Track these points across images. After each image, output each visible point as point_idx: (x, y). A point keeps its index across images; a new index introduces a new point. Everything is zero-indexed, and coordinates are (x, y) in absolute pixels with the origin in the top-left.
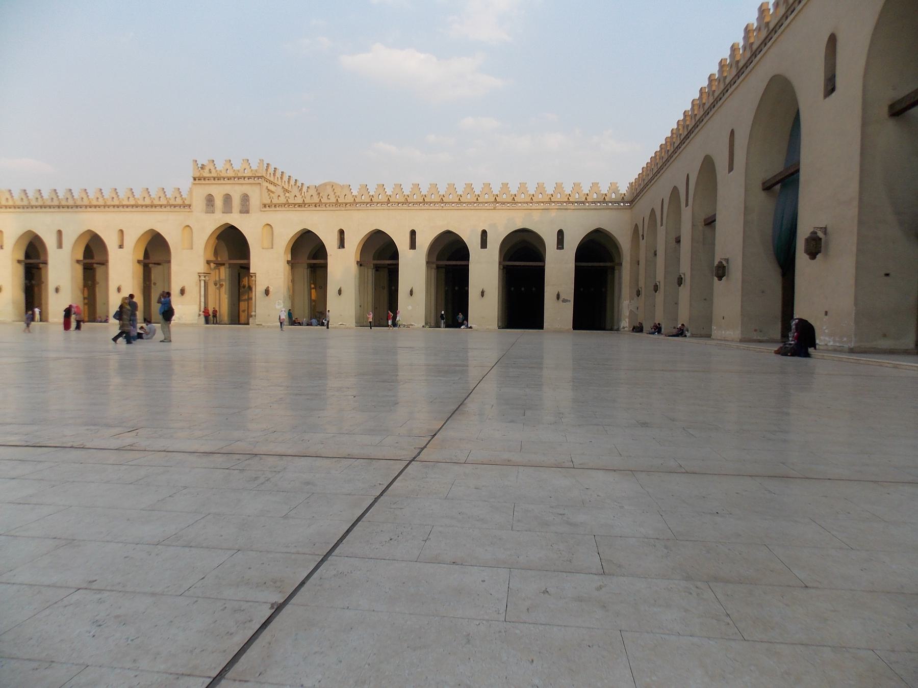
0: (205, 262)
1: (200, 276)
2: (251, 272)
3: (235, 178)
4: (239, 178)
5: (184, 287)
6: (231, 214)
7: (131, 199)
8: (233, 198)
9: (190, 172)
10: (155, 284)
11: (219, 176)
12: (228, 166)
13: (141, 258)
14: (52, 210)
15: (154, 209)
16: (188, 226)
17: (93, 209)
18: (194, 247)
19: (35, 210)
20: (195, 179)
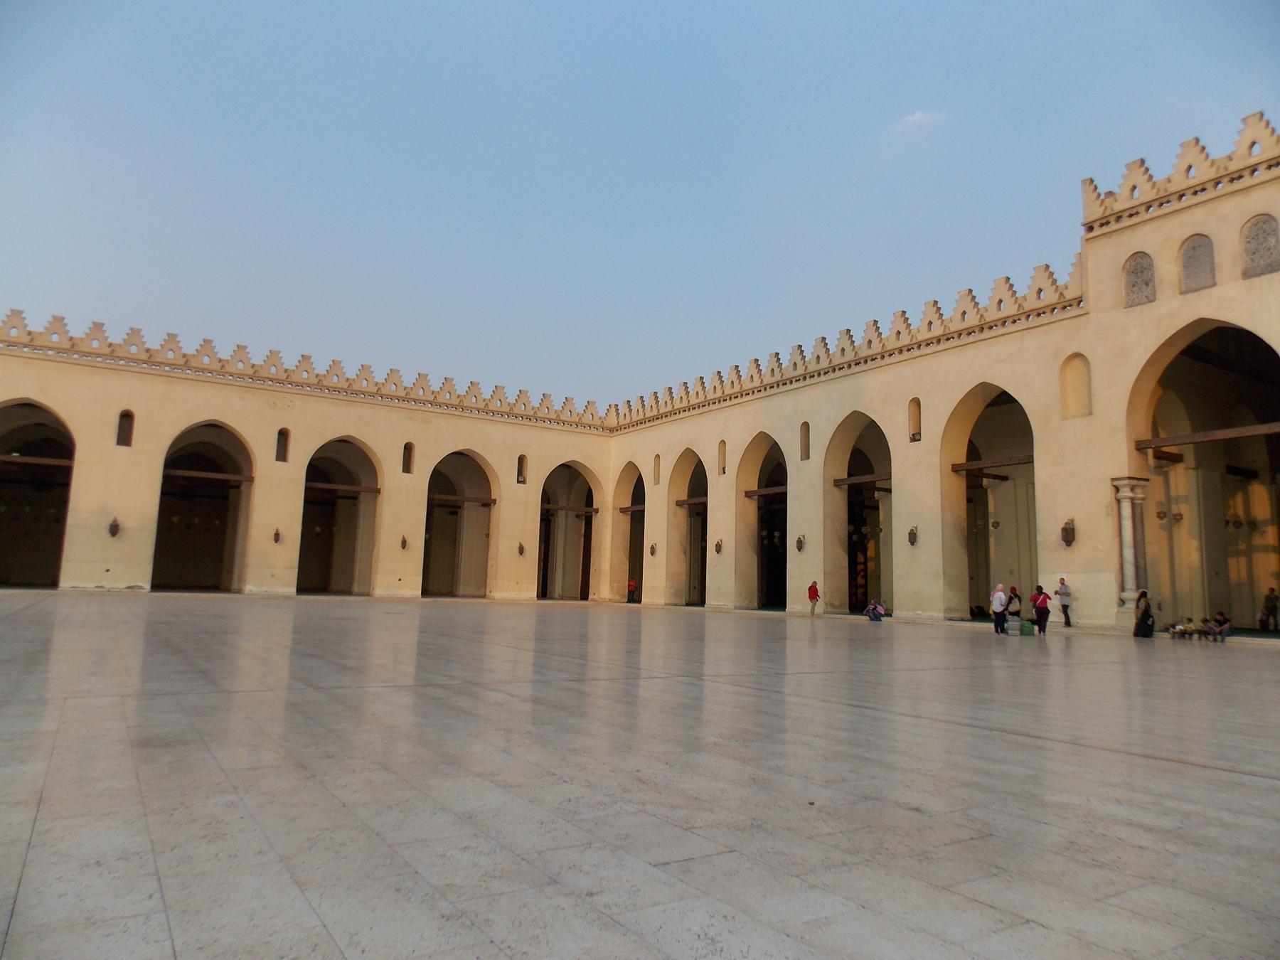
0: (1133, 444)
1: (1117, 489)
3: (1217, 182)
4: (1236, 177)
5: (1073, 521)
6: (1215, 288)
7: (936, 323)
8: (1213, 238)
9: (1077, 217)
10: (996, 525)
11: (1162, 194)
12: (1193, 156)
13: (961, 458)
14: (795, 385)
15: (986, 334)
16: (1077, 356)
17: (862, 367)
18: (1098, 406)
19: (769, 392)
20: (1090, 229)
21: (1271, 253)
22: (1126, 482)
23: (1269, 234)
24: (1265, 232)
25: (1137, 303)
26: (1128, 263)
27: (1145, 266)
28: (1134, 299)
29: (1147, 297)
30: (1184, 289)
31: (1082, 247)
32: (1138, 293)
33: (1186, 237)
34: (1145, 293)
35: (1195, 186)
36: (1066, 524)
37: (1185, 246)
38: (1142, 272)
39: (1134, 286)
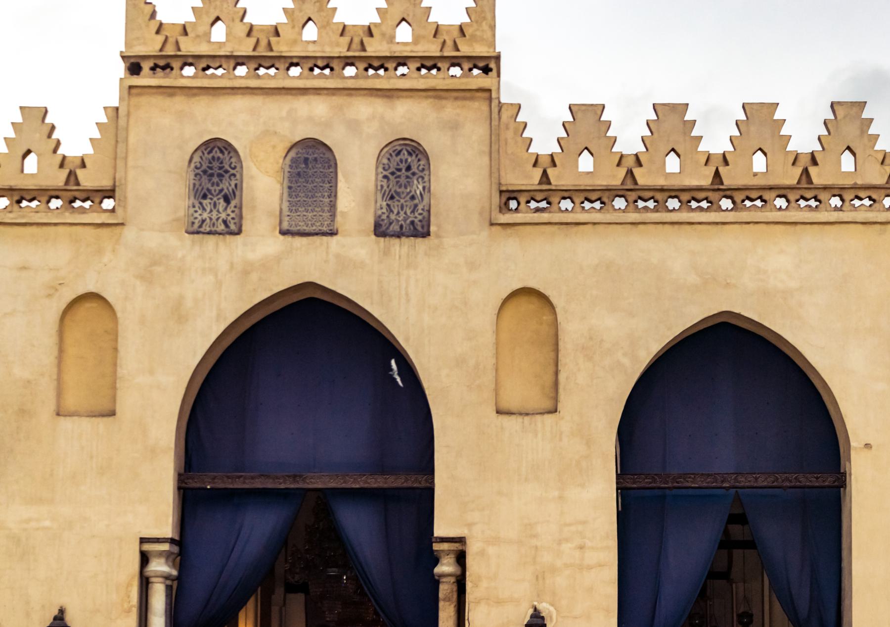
1: (145, 559)
2: (439, 530)
4: (380, 63)
6: (335, 238)
11: (262, 51)
20: (134, 68)
21: (416, 206)
22: (166, 547)
23: (414, 174)
24: (408, 168)
25: (208, 229)
26: (199, 153)
27: (227, 167)
28: (203, 221)
29: (225, 222)
30: (285, 226)
31: (121, 99)
32: (211, 211)
33: (298, 139)
34: (223, 216)
35: (316, 58)
36: (55, 618)
37: (292, 154)
38: (220, 176)
39: (205, 197)
